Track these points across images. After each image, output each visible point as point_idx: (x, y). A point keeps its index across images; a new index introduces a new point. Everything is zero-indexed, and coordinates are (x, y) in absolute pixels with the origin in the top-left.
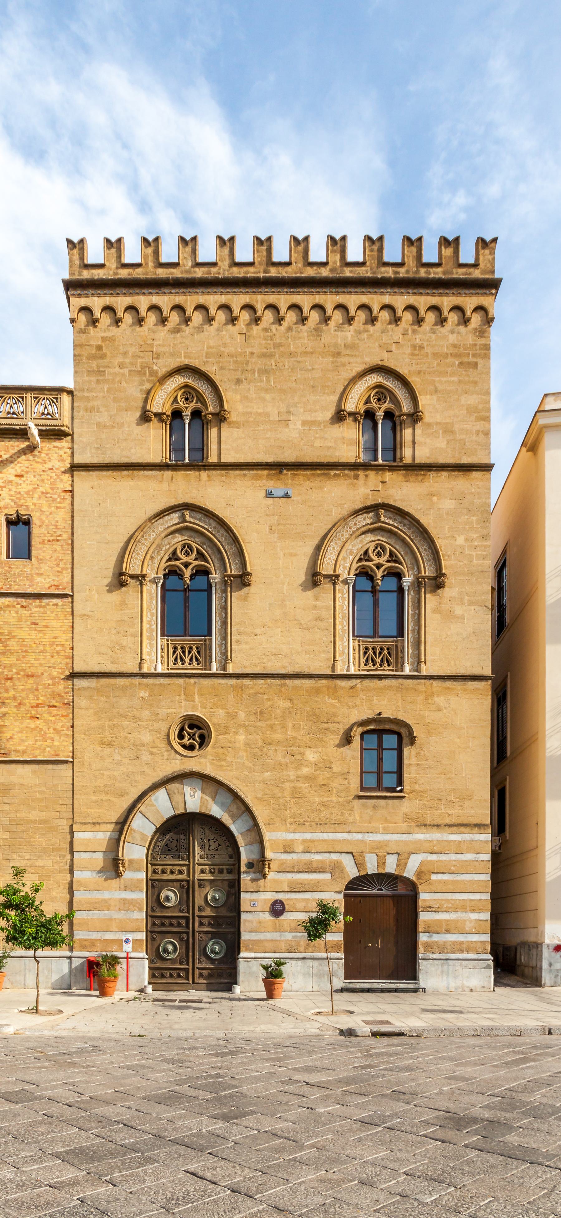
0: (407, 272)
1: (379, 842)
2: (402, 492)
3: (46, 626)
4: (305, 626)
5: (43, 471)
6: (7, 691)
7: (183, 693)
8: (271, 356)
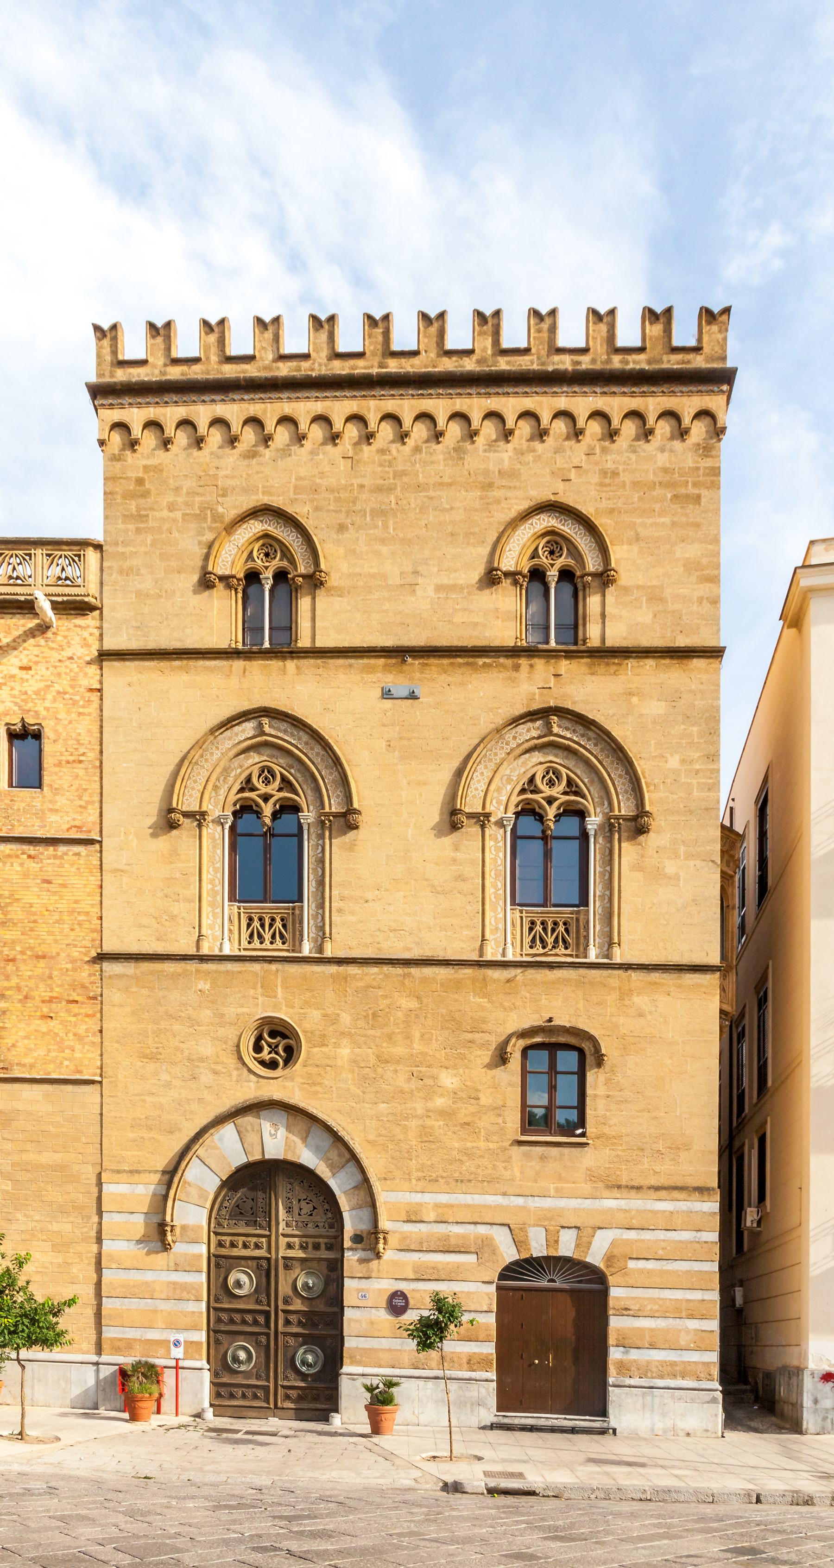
0: (594, 361)
1: (550, 1210)
2: (585, 689)
3: (64, 886)
4: (439, 889)
5: (60, 661)
6: (8, 978)
7: (259, 985)
8: (390, 489)
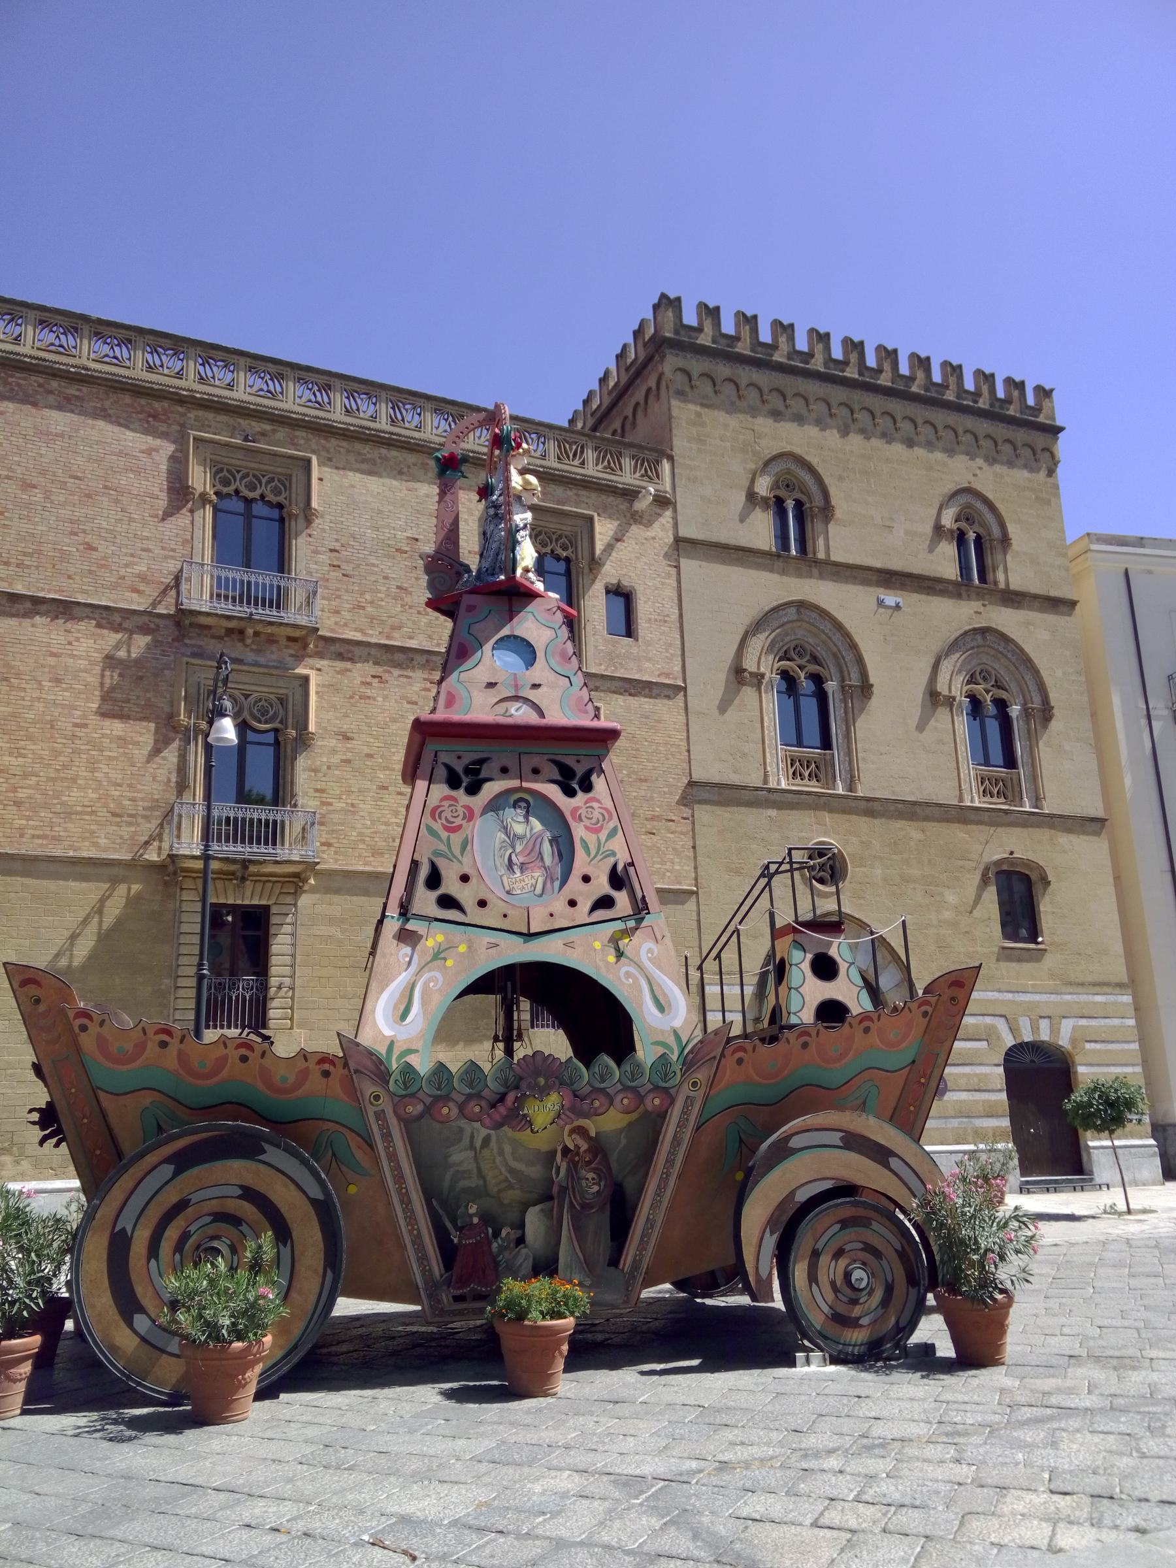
1: (1030, 1002)
3: (659, 721)
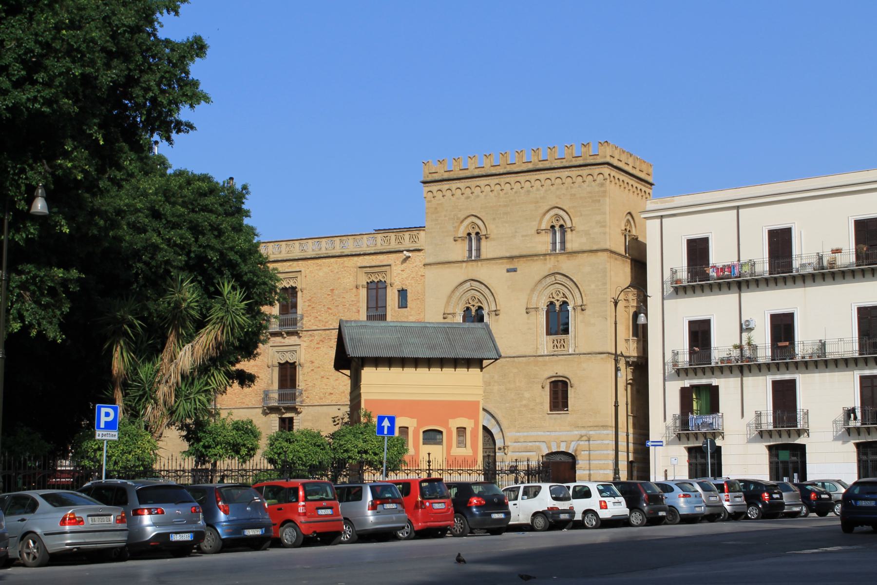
2: (566, 265)
